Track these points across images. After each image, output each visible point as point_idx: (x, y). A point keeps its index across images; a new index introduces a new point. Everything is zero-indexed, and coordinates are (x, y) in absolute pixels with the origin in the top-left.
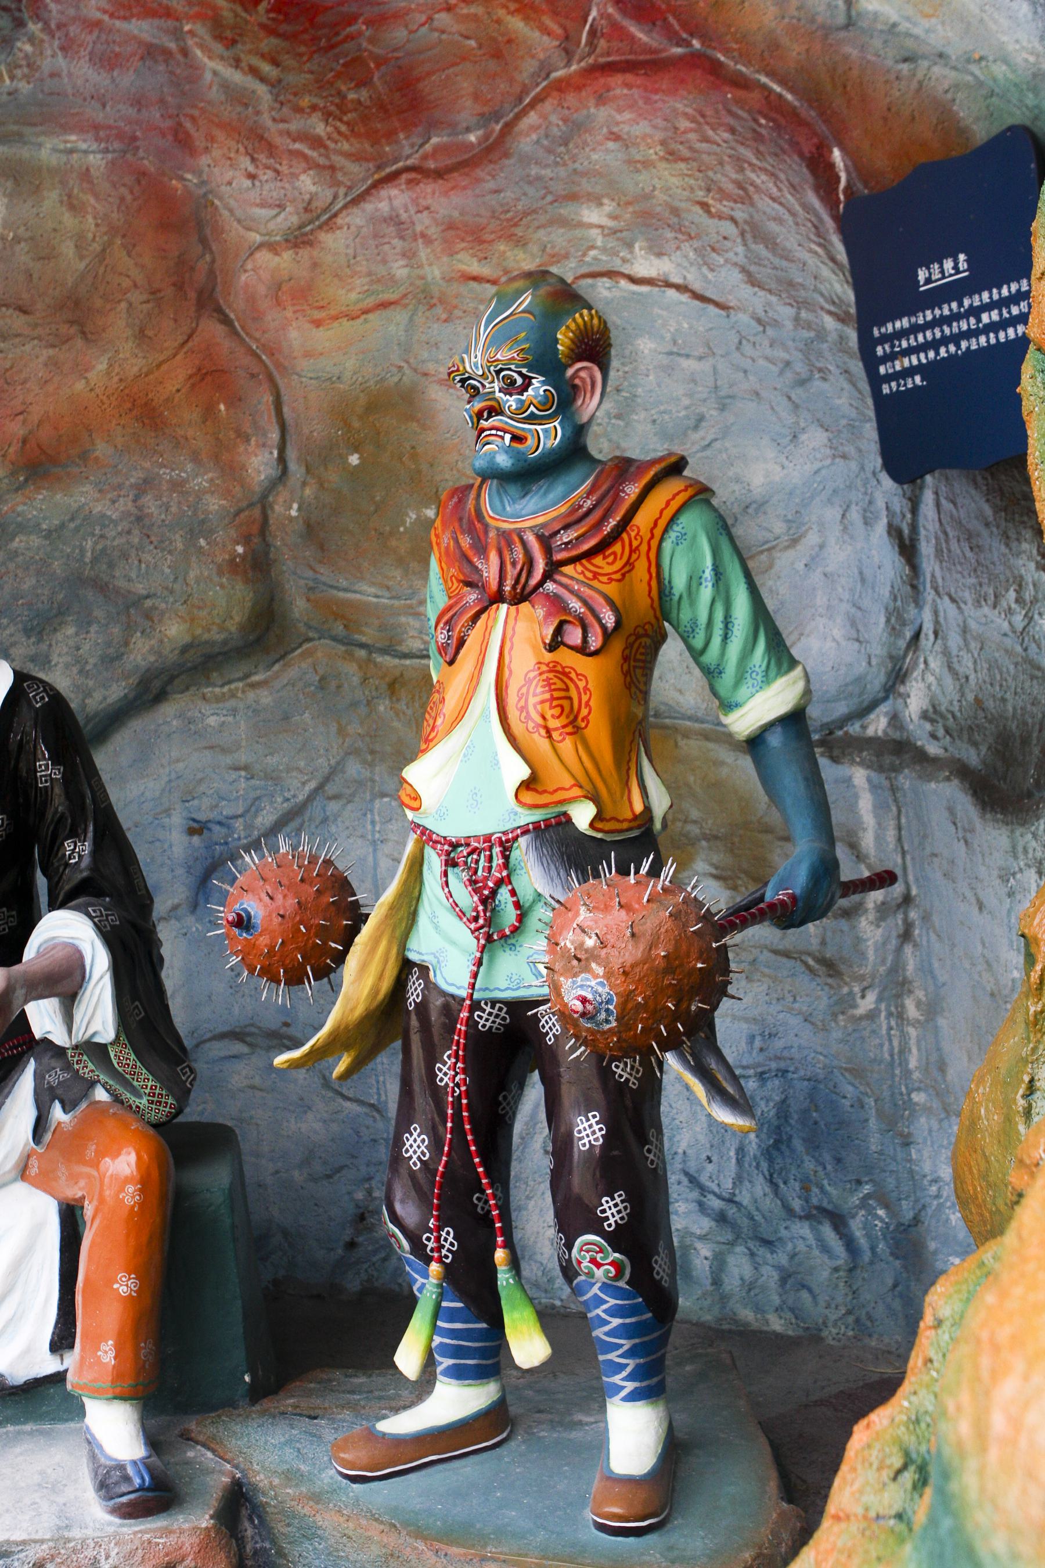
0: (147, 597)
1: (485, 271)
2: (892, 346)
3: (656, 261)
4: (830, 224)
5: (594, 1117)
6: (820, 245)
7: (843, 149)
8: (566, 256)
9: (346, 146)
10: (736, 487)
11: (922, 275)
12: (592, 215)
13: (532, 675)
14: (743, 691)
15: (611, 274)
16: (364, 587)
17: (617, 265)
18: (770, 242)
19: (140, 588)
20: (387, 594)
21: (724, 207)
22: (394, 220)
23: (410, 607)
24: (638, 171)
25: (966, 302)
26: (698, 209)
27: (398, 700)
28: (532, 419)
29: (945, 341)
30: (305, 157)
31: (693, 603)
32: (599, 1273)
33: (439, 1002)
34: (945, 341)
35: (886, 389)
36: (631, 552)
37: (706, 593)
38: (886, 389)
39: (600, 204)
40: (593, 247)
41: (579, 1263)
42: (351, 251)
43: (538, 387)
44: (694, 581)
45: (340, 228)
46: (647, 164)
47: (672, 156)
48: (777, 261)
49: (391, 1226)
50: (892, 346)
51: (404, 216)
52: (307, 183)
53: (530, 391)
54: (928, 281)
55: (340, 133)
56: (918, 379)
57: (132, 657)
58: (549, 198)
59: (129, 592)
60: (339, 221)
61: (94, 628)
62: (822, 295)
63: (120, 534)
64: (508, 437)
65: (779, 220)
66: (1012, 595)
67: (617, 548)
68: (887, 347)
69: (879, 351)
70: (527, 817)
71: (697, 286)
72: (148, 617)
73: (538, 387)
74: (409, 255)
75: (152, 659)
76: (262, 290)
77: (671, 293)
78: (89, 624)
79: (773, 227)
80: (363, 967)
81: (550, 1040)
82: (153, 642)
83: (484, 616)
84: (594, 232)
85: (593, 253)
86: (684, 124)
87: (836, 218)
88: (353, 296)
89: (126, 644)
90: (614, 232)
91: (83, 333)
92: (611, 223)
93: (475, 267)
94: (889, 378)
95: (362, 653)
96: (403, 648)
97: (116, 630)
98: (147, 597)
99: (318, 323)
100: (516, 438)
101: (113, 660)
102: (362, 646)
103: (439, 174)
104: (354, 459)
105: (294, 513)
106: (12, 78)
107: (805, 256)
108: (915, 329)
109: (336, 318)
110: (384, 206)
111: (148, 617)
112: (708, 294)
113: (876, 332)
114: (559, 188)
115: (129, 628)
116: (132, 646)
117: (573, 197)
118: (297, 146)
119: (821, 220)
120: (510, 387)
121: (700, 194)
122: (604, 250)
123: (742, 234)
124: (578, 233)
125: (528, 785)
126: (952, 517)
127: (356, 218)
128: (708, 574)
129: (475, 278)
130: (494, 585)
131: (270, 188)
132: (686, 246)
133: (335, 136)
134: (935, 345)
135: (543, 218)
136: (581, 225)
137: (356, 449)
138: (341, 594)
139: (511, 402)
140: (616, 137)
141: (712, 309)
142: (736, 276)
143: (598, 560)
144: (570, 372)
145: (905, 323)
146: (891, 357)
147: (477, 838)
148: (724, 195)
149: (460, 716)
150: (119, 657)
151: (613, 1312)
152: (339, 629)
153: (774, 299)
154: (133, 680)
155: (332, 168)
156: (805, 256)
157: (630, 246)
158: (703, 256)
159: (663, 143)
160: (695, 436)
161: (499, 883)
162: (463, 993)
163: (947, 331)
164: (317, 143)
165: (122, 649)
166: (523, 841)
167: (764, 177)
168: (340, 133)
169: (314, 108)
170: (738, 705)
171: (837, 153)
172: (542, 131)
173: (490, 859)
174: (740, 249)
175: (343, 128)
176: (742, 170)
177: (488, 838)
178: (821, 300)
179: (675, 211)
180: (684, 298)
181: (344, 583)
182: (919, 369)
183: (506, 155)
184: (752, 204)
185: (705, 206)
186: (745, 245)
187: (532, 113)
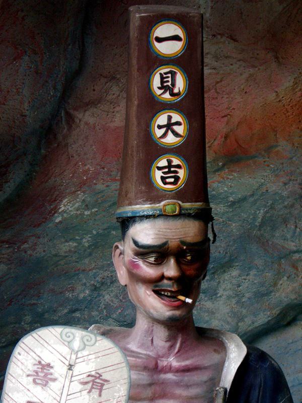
19: (292, 246)
57: (277, 295)
59: (283, 247)
61: (253, 272)
63: (285, 207)
72: (295, 267)
75: (293, 297)
78: (250, 269)
82: (295, 285)
89: (275, 285)
91: (277, 58)
97: (269, 275)
101: (263, 295)
111: (295, 267)
115: (279, 275)
116: (279, 286)
150: (268, 294)
154: (276, 311)
165: (272, 289)
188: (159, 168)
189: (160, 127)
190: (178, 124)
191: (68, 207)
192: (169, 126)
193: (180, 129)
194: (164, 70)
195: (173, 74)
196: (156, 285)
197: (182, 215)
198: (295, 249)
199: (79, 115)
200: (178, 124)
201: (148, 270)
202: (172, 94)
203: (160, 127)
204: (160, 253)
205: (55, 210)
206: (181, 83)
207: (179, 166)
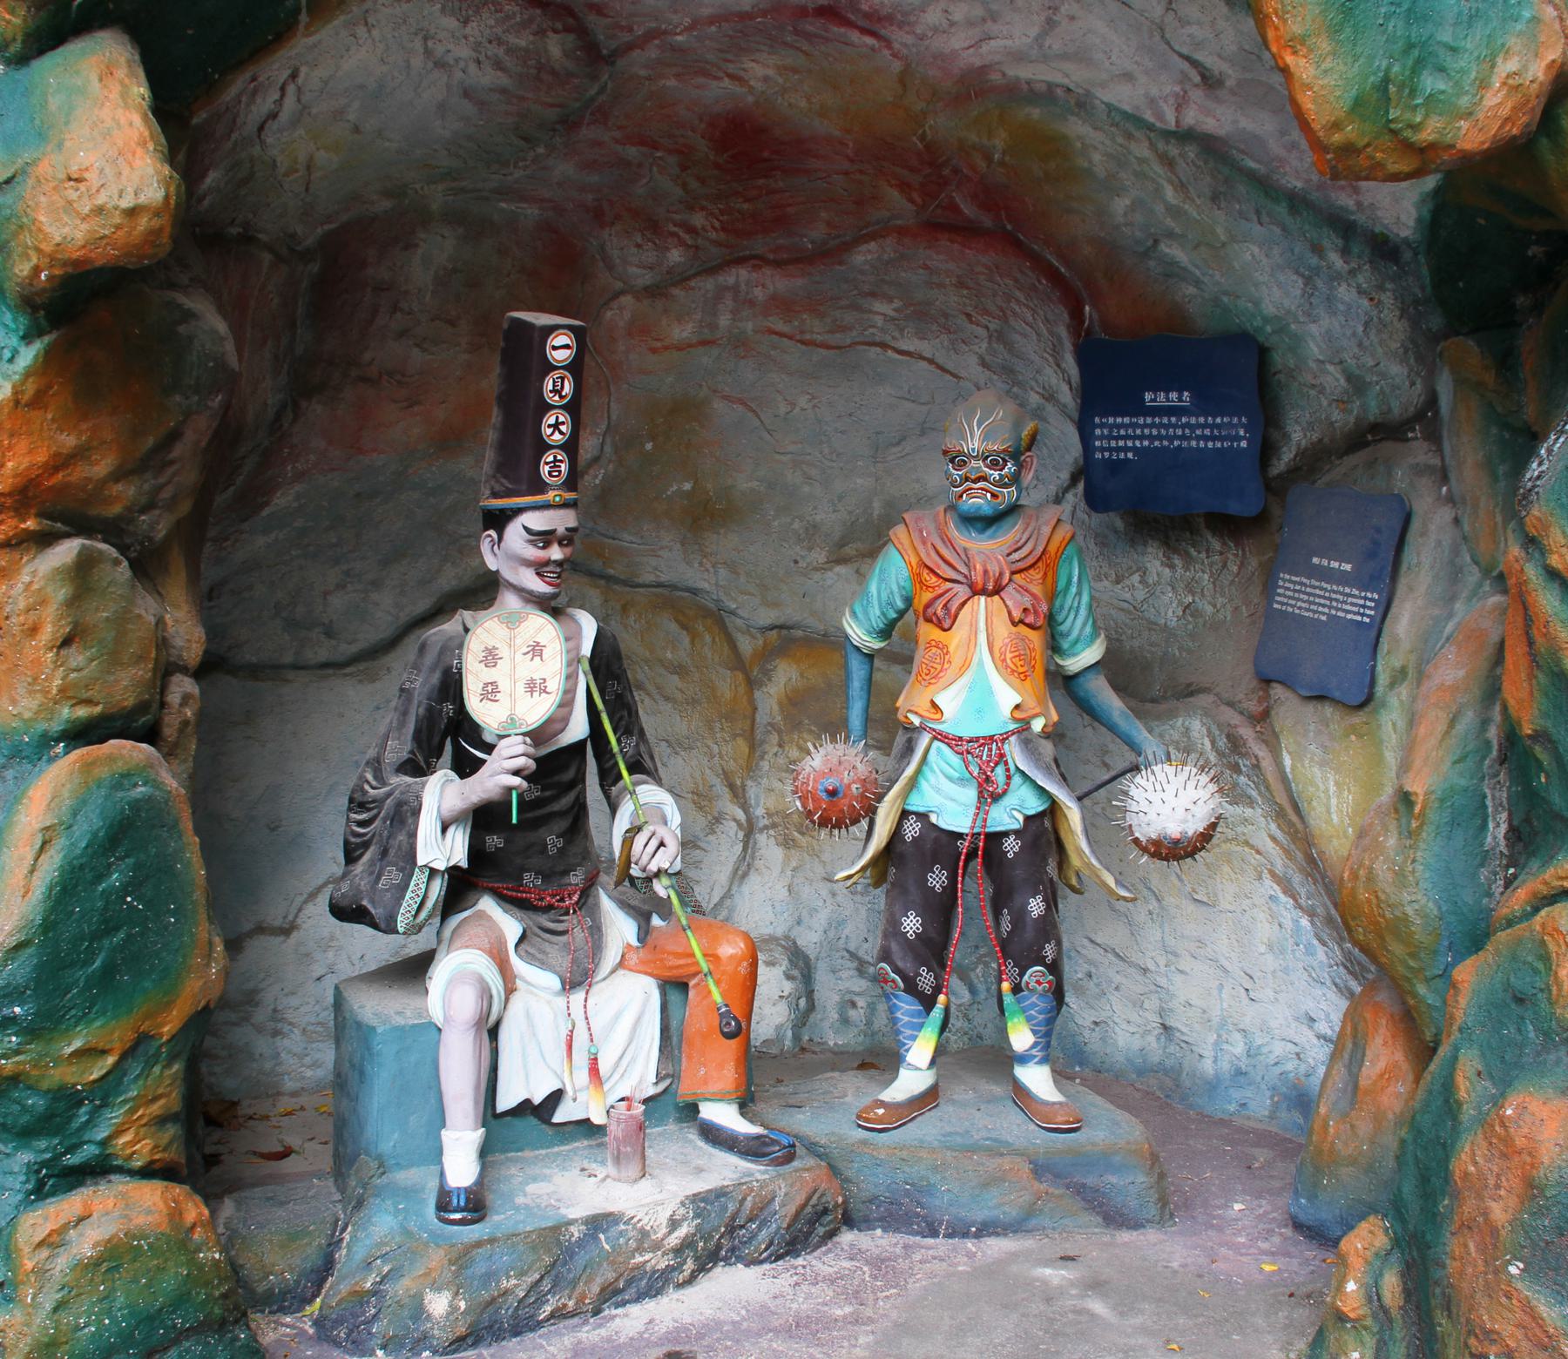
0: (465, 537)
1: (785, 328)
2: (1111, 432)
3: (916, 341)
4: (1068, 346)
5: (1039, 898)
6: (1052, 356)
7: (1093, 306)
8: (851, 329)
9: (713, 235)
10: (917, 486)
11: (1148, 396)
12: (880, 306)
13: (1007, 641)
14: (1079, 646)
15: (884, 346)
16: (626, 536)
17: (888, 339)
18: (1010, 347)
20: (639, 541)
21: (984, 320)
22: (735, 289)
23: (653, 550)
24: (932, 288)
25: (1184, 420)
26: (964, 317)
27: (628, 617)
28: (1005, 486)
29: (1160, 438)
30: (679, 236)
31: (1065, 595)
32: (1039, 988)
33: (934, 835)
34: (1160, 438)
35: (1098, 455)
36: (1047, 566)
37: (1074, 590)
38: (1098, 455)
39: (890, 300)
40: (873, 327)
41: (1028, 983)
42: (694, 306)
43: (1010, 468)
44: (1069, 582)
45: (692, 289)
46: (941, 286)
47: (961, 284)
48: (1007, 357)
49: (893, 975)
50: (1111, 432)
51: (743, 287)
52: (675, 256)
53: (1006, 470)
54: (1152, 401)
55: (713, 227)
56: (1130, 455)
58: (855, 292)
60: (693, 283)
62: (1037, 381)
64: (989, 495)
65: (1025, 336)
66: (1136, 578)
67: (1040, 564)
68: (1106, 432)
69: (1098, 432)
70: (1012, 726)
71: (940, 361)
73: (1010, 468)
74: (735, 312)
75: (454, 583)
76: (621, 324)
77: (924, 364)
79: (1017, 337)
80: (887, 815)
81: (1010, 855)
83: (970, 602)
84: (879, 321)
85: (871, 330)
86: (979, 269)
87: (1075, 345)
88: (685, 334)
90: (894, 319)
92: (892, 313)
93: (780, 326)
94: (1103, 449)
95: (603, 582)
96: (640, 581)
98: (465, 537)
99: (654, 351)
100: (994, 496)
102: (609, 579)
103: (778, 264)
104: (649, 446)
105: (597, 482)
106: (515, 167)
107: (1036, 358)
108: (1134, 426)
109: (666, 348)
110: (731, 280)
112: (947, 367)
113: (1097, 420)
114: (866, 288)
117: (873, 295)
118: (676, 229)
119: (1061, 343)
120: (994, 465)
121: (969, 309)
122: (882, 330)
123: (990, 337)
124: (866, 316)
125: (1017, 707)
126: (1083, 522)
127: (709, 284)
128: (1075, 579)
129: (776, 333)
130: (980, 586)
131: (650, 256)
132: (944, 337)
133: (709, 228)
134: (1151, 438)
135: (844, 302)
136: (870, 312)
137: (653, 438)
138: (606, 540)
139: (996, 475)
140: (926, 267)
141: (948, 377)
142: (973, 361)
143: (1031, 571)
144: (1023, 458)
145: (1127, 420)
146: (1110, 437)
147: (984, 738)
148: (986, 312)
149: (965, 666)
151: (1040, 1013)
152: (597, 565)
153: (995, 377)
155: (697, 247)
156: (1036, 358)
157: (901, 330)
158: (953, 344)
159: (958, 277)
160: (894, 450)
161: (997, 764)
162: (966, 831)
163: (1163, 432)
164: (692, 230)
166: (1013, 739)
167: (1025, 310)
168: (713, 227)
169: (703, 208)
170: (1075, 655)
171: (1087, 308)
172: (876, 256)
173: (990, 750)
174: (984, 345)
175: (717, 224)
176: (1009, 302)
177: (991, 738)
178: (1033, 383)
179: (946, 316)
180: (932, 368)
181: (611, 532)
182: (1134, 449)
183: (840, 263)
184: (1006, 322)
185: (968, 316)
186: (989, 343)
187: (873, 243)
188: (547, 463)
189: (549, 426)
190: (563, 423)
191: (282, 500)
192: (556, 426)
193: (563, 428)
194: (556, 374)
195: (563, 379)
196: (540, 568)
197: (564, 505)
198: (466, 533)
199: (304, 404)
200: (563, 423)
201: (532, 553)
202: (562, 397)
203: (549, 426)
204: (545, 538)
205: (267, 504)
206: (568, 388)
207: (561, 461)
